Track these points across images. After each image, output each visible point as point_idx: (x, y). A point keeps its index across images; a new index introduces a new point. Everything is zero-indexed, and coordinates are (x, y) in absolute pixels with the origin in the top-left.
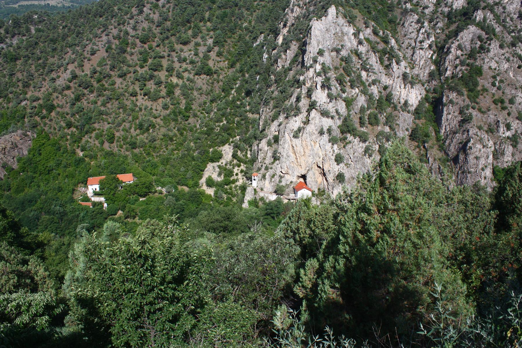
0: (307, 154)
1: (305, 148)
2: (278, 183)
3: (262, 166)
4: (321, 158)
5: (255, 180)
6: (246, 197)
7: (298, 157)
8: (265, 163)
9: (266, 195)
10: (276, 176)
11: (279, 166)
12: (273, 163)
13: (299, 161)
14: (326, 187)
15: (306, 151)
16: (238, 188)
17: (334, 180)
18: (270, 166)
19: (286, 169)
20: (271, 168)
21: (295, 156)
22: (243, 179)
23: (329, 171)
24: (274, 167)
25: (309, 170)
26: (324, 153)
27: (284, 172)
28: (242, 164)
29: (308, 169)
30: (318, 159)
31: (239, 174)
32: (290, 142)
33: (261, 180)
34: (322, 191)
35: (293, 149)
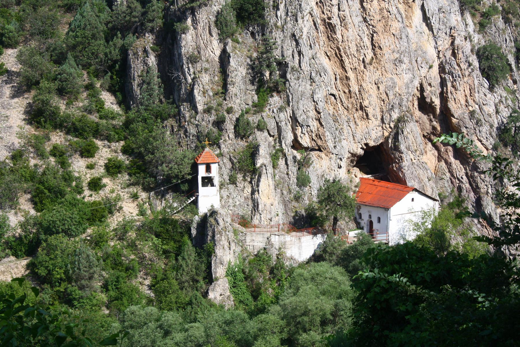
0: (388, 55)
1: (379, 27)
2: (294, 187)
3: (219, 123)
4: (436, 69)
5: (208, 181)
6: (219, 251)
7: (351, 75)
8: (229, 111)
9: (275, 240)
10: (281, 162)
11: (284, 117)
12: (259, 107)
13: (355, 88)
14: (466, 185)
15: (384, 40)
16: (132, 235)
17: (495, 148)
18: (254, 119)
19: (313, 125)
20: (261, 127)
21: (339, 71)
22: (135, 197)
23: (472, 114)
24: (271, 125)
25: (399, 120)
26: (444, 43)
27: (305, 141)
28: (99, 143)
29: (395, 115)
30: (424, 71)
31: (105, 181)
32: (317, 12)
33: (233, 181)
34: (451, 206)
35: (330, 38)
